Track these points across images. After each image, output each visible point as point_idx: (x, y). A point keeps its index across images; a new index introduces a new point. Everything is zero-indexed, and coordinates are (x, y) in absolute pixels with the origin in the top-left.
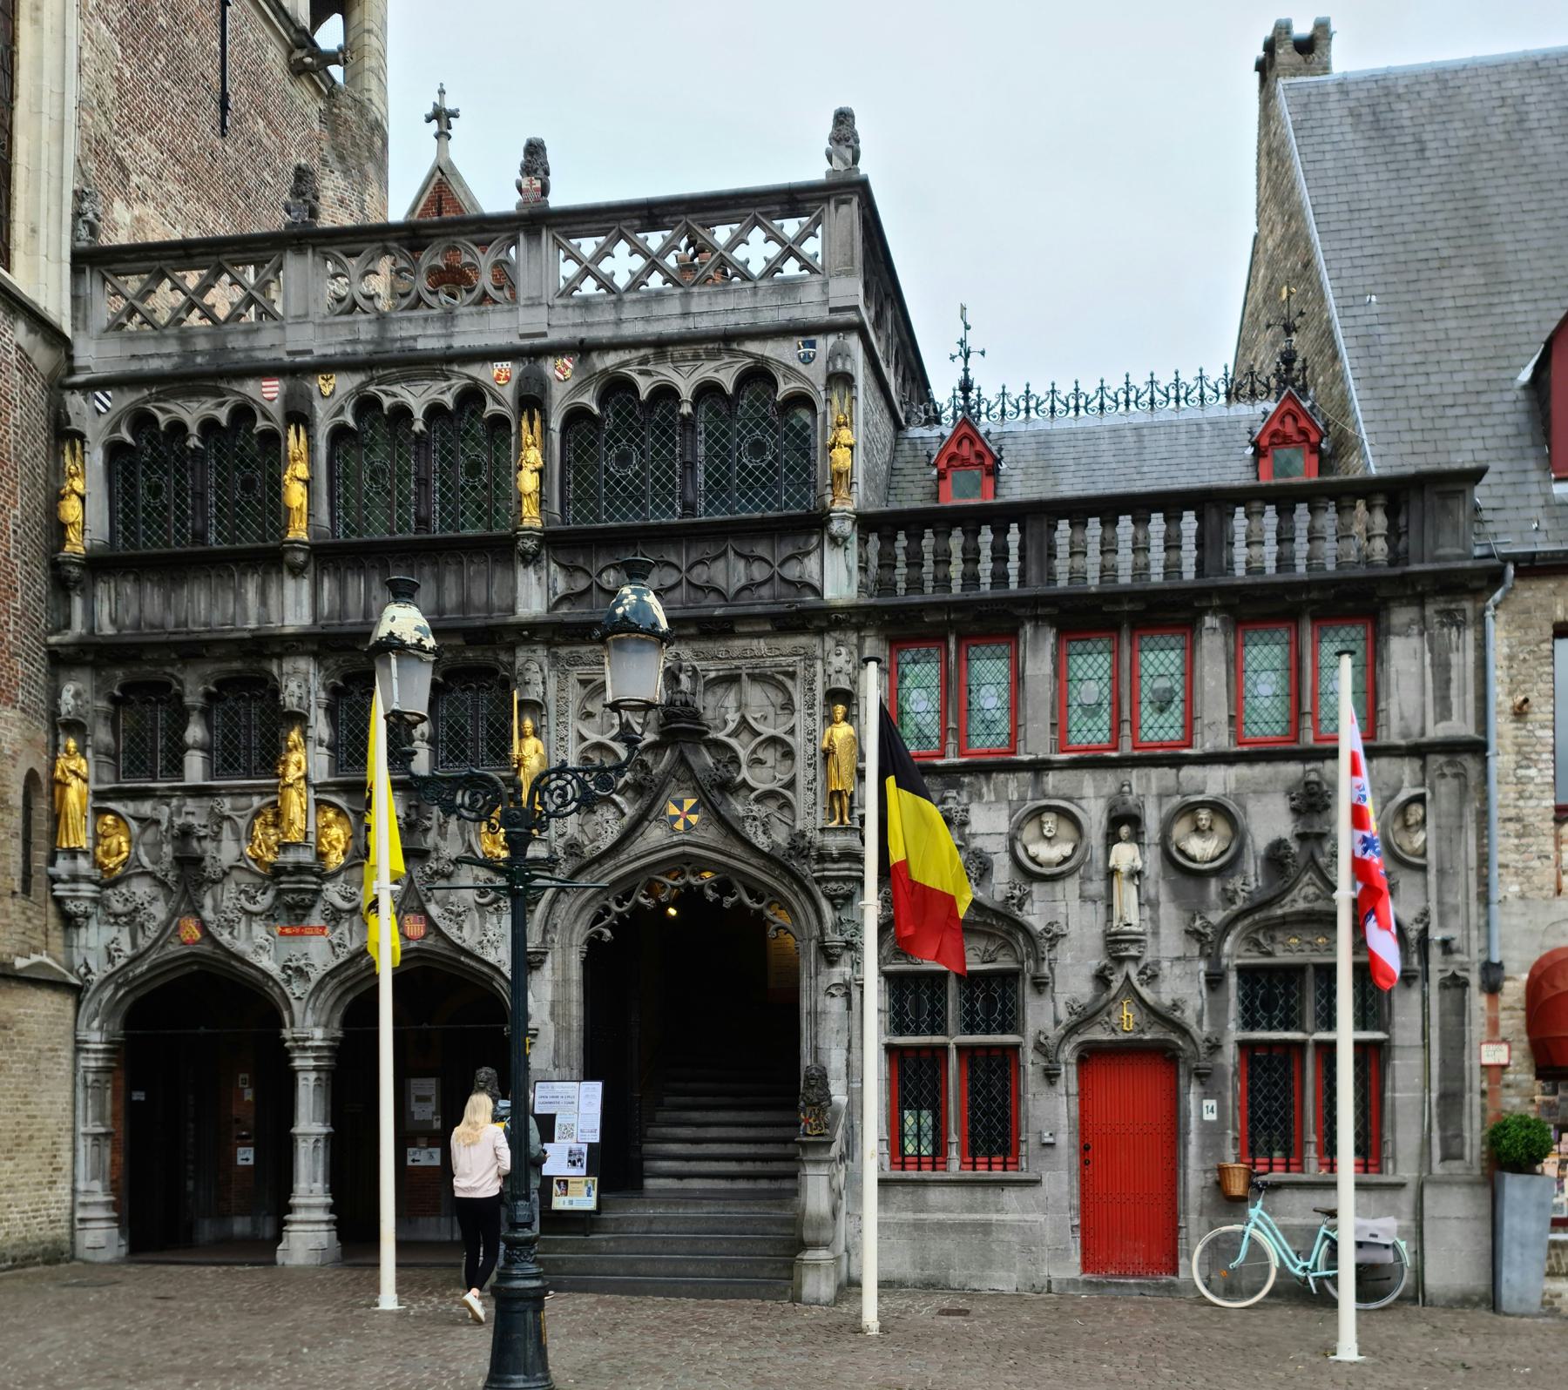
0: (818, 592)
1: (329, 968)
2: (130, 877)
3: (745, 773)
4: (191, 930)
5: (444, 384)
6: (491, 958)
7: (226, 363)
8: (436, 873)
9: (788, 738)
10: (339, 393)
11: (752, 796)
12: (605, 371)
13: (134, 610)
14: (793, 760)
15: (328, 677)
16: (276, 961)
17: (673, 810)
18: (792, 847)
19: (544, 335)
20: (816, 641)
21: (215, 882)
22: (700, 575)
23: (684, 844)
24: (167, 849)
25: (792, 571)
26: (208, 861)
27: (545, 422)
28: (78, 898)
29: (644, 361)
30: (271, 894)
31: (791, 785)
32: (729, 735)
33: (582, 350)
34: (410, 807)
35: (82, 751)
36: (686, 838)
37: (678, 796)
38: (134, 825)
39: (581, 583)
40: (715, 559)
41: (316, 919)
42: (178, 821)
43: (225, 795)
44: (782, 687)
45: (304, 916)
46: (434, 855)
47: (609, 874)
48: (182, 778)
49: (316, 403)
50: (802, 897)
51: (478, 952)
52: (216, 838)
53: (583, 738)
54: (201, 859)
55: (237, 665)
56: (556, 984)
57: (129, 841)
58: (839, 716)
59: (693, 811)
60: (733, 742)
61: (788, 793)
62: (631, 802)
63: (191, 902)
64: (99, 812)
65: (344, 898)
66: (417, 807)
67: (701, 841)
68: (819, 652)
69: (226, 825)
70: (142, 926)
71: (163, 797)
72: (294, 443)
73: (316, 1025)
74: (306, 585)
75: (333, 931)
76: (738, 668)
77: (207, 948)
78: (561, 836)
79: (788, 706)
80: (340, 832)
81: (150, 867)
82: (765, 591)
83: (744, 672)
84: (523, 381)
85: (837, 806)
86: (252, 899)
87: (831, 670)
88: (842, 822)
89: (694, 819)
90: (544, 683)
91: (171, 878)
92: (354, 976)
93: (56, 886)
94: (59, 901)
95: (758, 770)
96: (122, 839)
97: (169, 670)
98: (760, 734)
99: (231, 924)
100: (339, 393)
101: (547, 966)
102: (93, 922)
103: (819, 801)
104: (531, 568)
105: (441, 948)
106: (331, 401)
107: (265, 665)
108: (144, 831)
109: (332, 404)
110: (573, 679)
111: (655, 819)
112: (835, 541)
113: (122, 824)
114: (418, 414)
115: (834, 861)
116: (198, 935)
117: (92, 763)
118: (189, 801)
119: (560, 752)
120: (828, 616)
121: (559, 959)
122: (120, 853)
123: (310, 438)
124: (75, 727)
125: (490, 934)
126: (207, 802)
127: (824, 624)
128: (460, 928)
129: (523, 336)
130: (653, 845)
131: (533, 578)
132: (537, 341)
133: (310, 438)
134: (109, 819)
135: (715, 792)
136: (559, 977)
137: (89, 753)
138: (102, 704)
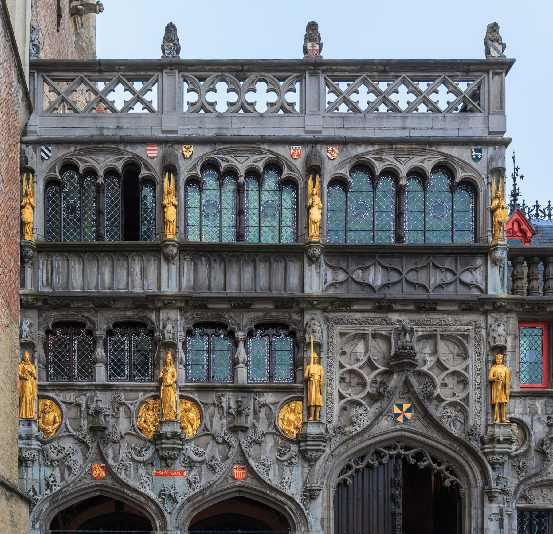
0: (484, 291)
1: (188, 496)
2: (60, 437)
4: (99, 471)
5: (259, 156)
7: (123, 133)
8: (254, 441)
10: (195, 157)
11: (443, 404)
12: (357, 156)
13: (63, 279)
15: (186, 324)
16: (153, 491)
17: (396, 410)
19: (320, 132)
20: (482, 318)
21: (115, 442)
22: (412, 277)
23: (402, 430)
24: (85, 423)
25: (467, 277)
26: (110, 429)
27: (321, 182)
28: (30, 449)
29: (380, 152)
30: (150, 452)
31: (466, 399)
33: (344, 143)
34: (237, 402)
36: (404, 426)
37: (399, 402)
38: (64, 407)
39: (341, 277)
40: (422, 268)
41: (178, 466)
42: (92, 406)
43: (121, 391)
44: (460, 344)
45: (172, 464)
46: (250, 431)
47: (358, 445)
48: (93, 379)
49: (180, 162)
50: (473, 463)
51: (280, 488)
52: (116, 416)
53: (342, 366)
54: (106, 428)
55: (129, 313)
57: (62, 415)
59: (408, 411)
62: (371, 406)
63: (100, 453)
64: (40, 397)
65: (196, 454)
66: (241, 402)
67: (413, 428)
69: (122, 409)
70: (69, 468)
71: (82, 390)
72: (168, 184)
74: (174, 268)
75: (190, 472)
77: (109, 482)
78: (330, 422)
79: (464, 355)
80: (194, 415)
81: (74, 433)
82: (451, 288)
83: (439, 333)
84: (308, 158)
86: (140, 453)
89: (409, 416)
91: (88, 439)
96: (56, 415)
97: (86, 314)
98: (447, 369)
99: (126, 468)
100: (195, 157)
101: (320, 499)
102: (36, 464)
105: (255, 485)
106: (190, 161)
107: (148, 314)
108: (69, 410)
109: (190, 163)
112: (495, 263)
113: (54, 404)
114: (242, 173)
116: (103, 474)
118: (98, 393)
119: (329, 374)
121: (326, 494)
122: (54, 423)
123: (177, 181)
125: (287, 478)
126: (108, 394)
128: (267, 474)
129: (307, 132)
130: (384, 430)
131: (314, 272)
132: (317, 136)
133: (177, 181)
134: (48, 402)
136: (325, 505)
138: (42, 333)
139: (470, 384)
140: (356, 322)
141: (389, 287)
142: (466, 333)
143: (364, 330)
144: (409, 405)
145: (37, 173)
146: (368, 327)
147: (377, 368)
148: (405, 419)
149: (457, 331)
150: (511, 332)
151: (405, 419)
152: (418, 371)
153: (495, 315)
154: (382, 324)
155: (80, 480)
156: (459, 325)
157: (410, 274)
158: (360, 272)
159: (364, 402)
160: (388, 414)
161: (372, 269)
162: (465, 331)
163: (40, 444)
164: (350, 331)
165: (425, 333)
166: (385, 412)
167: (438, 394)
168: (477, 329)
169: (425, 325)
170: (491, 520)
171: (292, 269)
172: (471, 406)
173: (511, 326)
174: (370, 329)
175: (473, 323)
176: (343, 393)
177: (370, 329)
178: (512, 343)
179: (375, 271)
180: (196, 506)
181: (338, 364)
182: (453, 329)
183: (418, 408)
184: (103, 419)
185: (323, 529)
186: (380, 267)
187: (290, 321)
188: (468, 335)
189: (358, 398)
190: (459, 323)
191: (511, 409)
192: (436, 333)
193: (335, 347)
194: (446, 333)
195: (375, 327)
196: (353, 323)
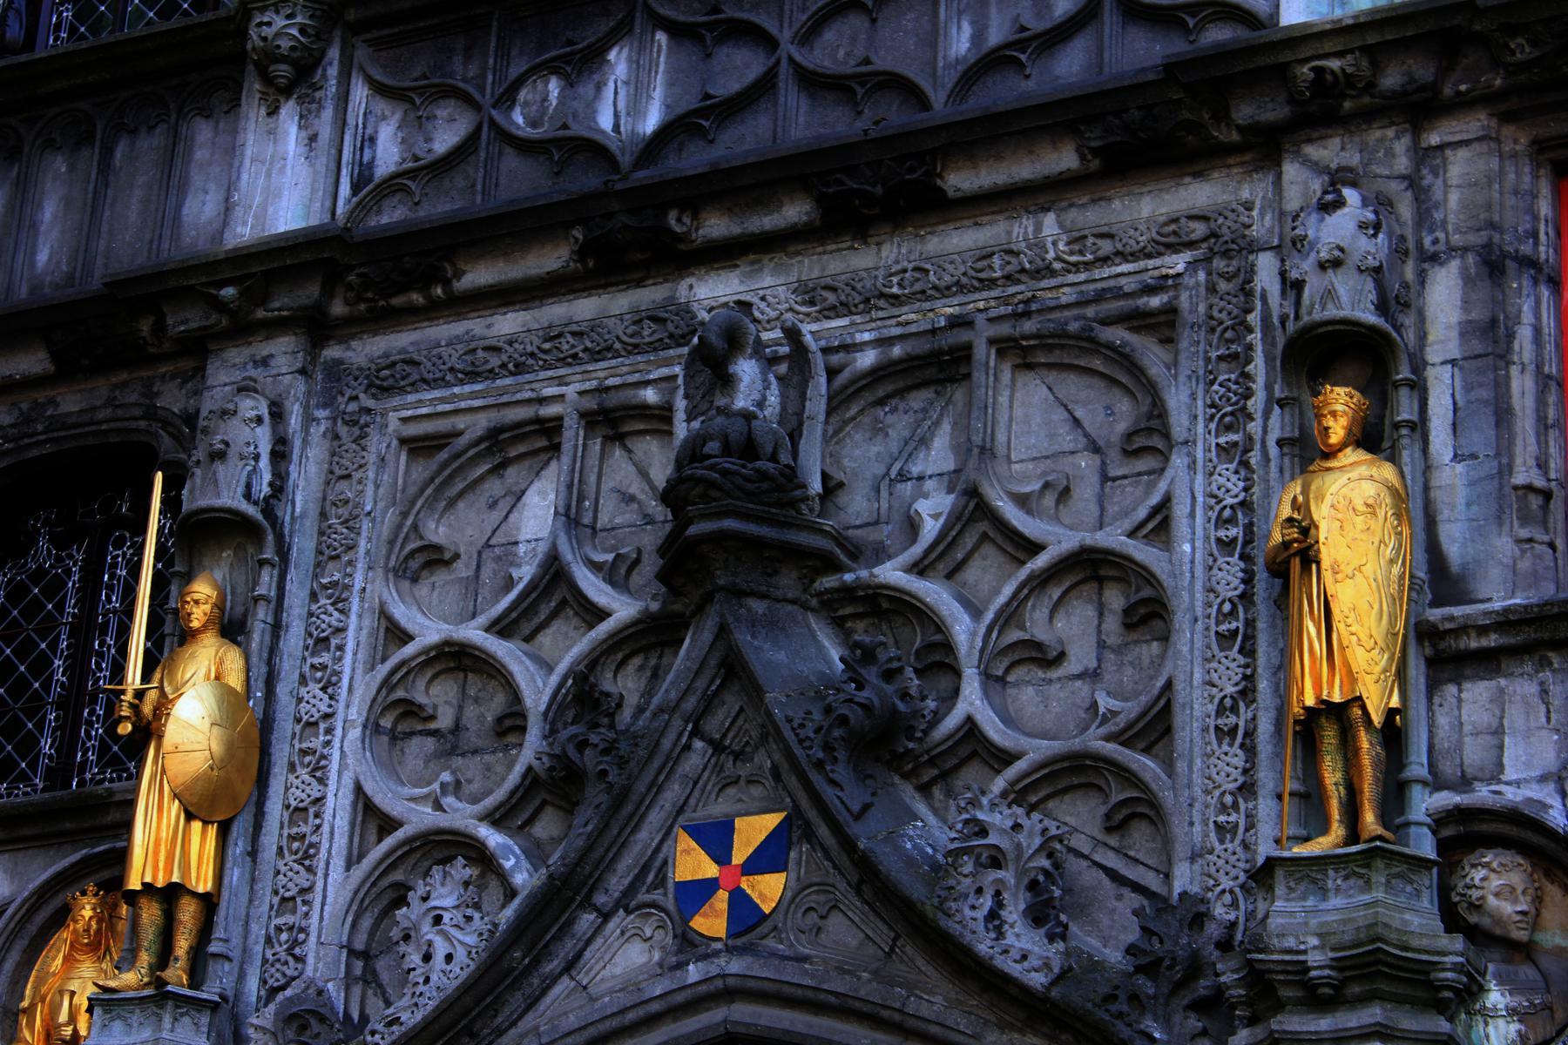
3: (972, 700)
9: (1142, 552)
11: (999, 784)
14: (1165, 638)
17: (693, 863)
18: (1145, 962)
20: (1254, 189)
23: (729, 992)
32: (920, 568)
36: (736, 966)
37: (717, 809)
39: (444, 139)
53: (397, 634)
58: (1337, 431)
59: (766, 858)
60: (934, 592)
67: (791, 974)
68: (1262, 226)
76: (958, 322)
85: (1332, 776)
87: (1303, 267)
88: (1353, 836)
89: (768, 889)
90: (280, 455)
95: (1027, 696)
98: (1035, 548)
103: (1265, 776)
104: (289, 112)
111: (624, 903)
115: (1318, 999)
120: (1282, 73)
127: (1273, 111)
135: (842, 772)
139: (1181, 620)
140: (495, 361)
141: (701, 132)
142: (1155, 302)
143: (542, 401)
144: (772, 821)
146: (561, 380)
147: (601, 614)
148: (744, 913)
149: (1099, 297)
150: (1456, 239)
151: (744, 913)
152: (848, 593)
153: (1331, 151)
154: (636, 349)
156: (1105, 260)
157: (828, 36)
158: (554, 87)
159: (493, 838)
160: (643, 897)
161: (619, 61)
162: (1150, 290)
165: (897, 351)
166: (617, 882)
167: (969, 719)
168: (1219, 264)
169: (895, 300)
171: (200, 154)
172: (1181, 766)
173: (1454, 198)
174: (570, 391)
175: (1199, 229)
176: (388, 798)
177: (570, 391)
178: (1466, 304)
179: (635, 64)
182: (1068, 295)
183: (823, 831)
186: (661, 37)
187: (156, 426)
188: (1171, 311)
189: (462, 816)
190: (1106, 247)
191: (1474, 753)
192: (963, 336)
193: (366, 525)
194: (1029, 326)
195: (602, 372)
196: (472, 375)
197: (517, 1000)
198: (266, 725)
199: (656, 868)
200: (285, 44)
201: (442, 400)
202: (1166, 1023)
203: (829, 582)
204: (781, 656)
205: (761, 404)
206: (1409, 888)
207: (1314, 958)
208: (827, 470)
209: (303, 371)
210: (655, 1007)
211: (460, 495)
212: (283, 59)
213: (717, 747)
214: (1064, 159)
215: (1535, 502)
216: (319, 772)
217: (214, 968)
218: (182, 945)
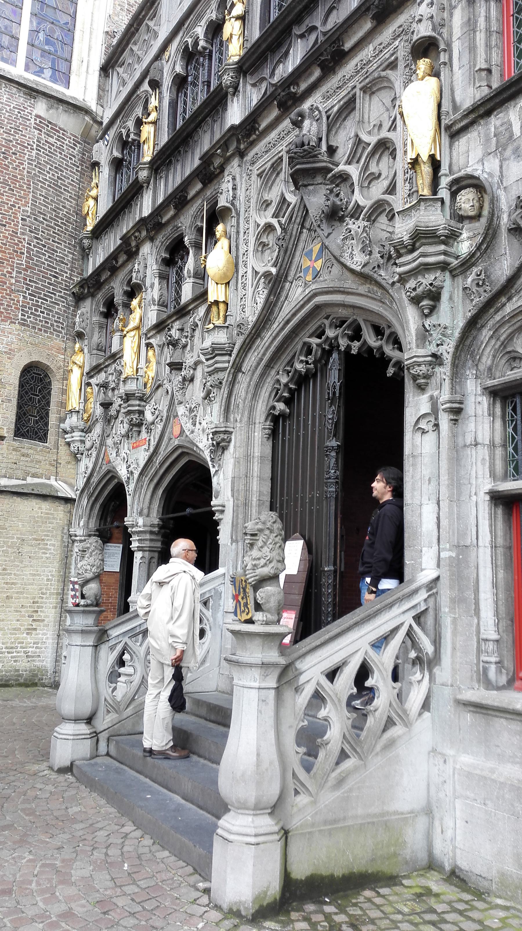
6: (201, 446)
15: (158, 253)
23: (315, 295)
35: (82, 350)
36: (313, 287)
56: (237, 461)
61: (387, 197)
72: (153, 102)
73: (141, 514)
90: (234, 189)
92: (156, 473)
93: (66, 436)
94: (68, 444)
110: (254, 177)
117: (87, 355)
123: (160, 93)
124: (80, 335)
133: (160, 93)
137: (86, 350)
138: (96, 318)
145: (102, 163)
155: (101, 468)
163: (84, 434)
164: (266, 166)
166: (292, 273)
170: (424, 432)
174: (284, 147)
180: (155, 481)
181: (253, 224)
184: (110, 393)
185: (233, 496)
197: (277, 309)
198: (237, 257)
199: (299, 268)
200: (228, 82)
201: (263, 161)
202: (387, 270)
203: (330, 175)
204: (316, 199)
205: (309, 131)
206: (433, 209)
207: (406, 238)
208: (331, 143)
209: (239, 166)
210: (302, 303)
211: (272, 185)
212: (230, 87)
213: (309, 230)
214: (368, 25)
215: (484, 74)
216: (245, 265)
217: (228, 318)
218: (222, 314)
